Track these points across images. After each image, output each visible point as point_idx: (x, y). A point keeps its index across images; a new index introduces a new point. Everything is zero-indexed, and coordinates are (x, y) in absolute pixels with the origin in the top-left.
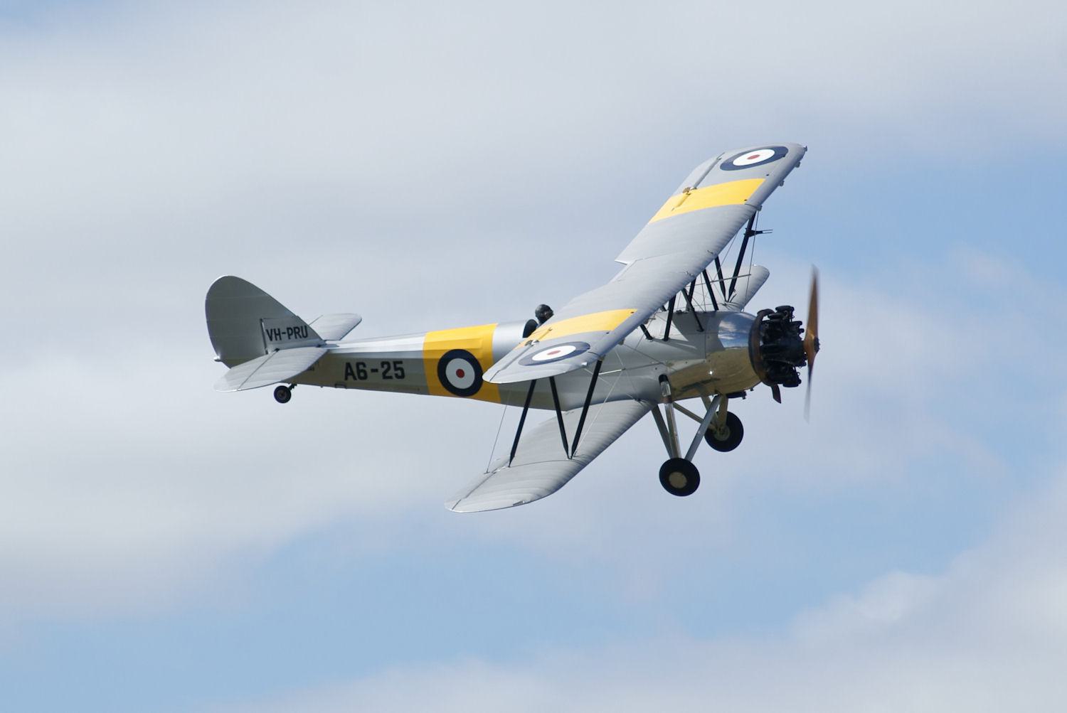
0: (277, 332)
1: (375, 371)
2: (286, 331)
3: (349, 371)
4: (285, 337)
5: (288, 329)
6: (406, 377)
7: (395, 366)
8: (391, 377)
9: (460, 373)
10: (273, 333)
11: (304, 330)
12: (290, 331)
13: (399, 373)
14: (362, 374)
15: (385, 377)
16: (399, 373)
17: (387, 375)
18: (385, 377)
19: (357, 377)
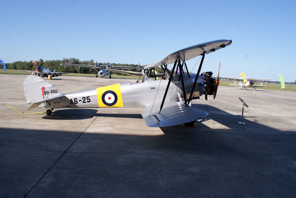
0: (47, 92)
1: (81, 100)
2: (50, 91)
3: (72, 102)
4: (50, 93)
8: (86, 102)
9: (110, 98)
10: (46, 93)
11: (56, 91)
12: (52, 91)
13: (89, 100)
14: (76, 102)
15: (84, 102)
16: (89, 100)
17: (84, 102)
18: (84, 102)
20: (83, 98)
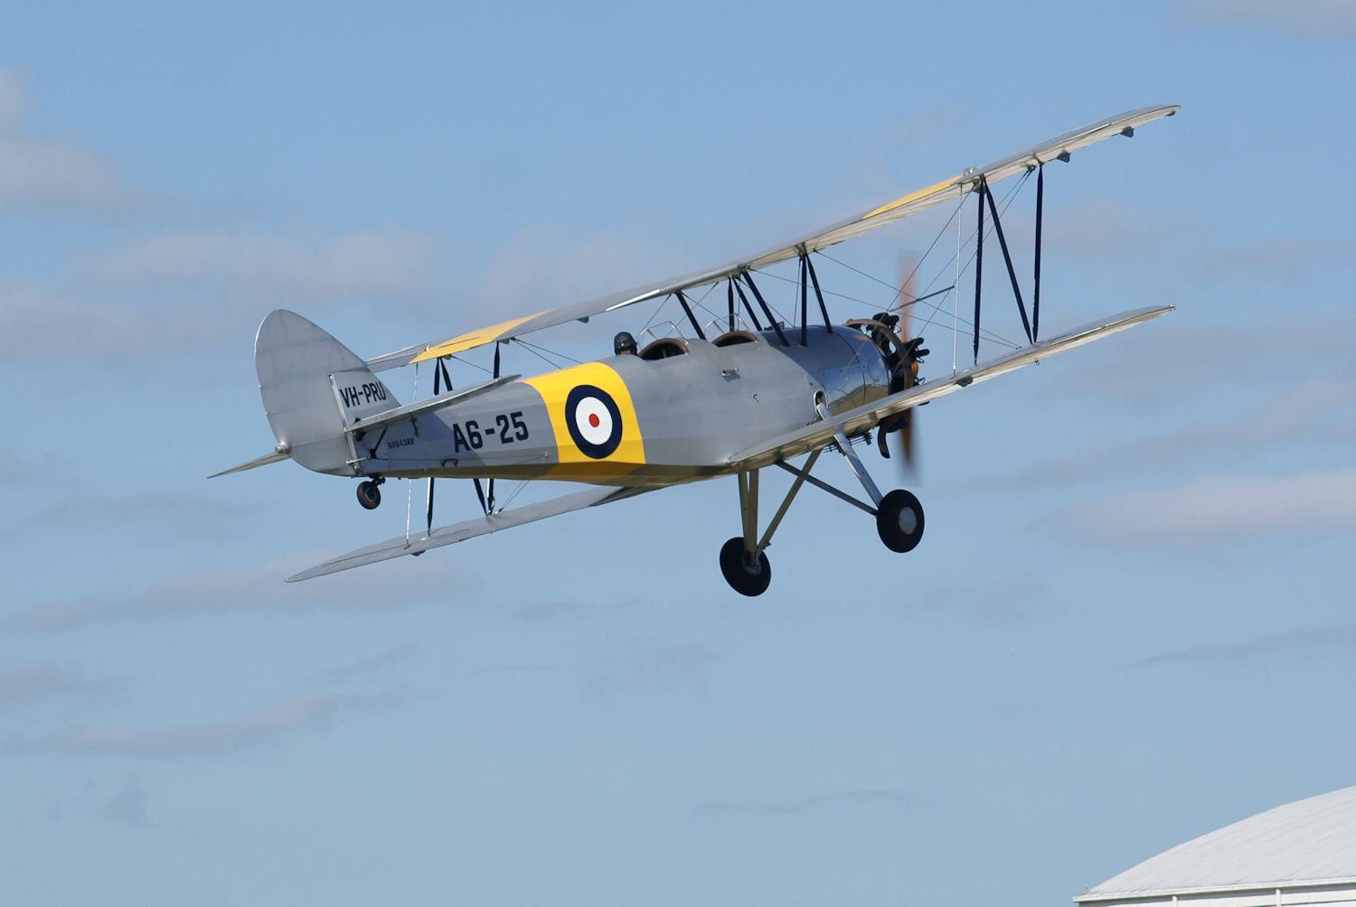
0: (353, 393)
1: (490, 432)
2: (362, 390)
4: (362, 398)
5: (364, 386)
6: (529, 435)
7: (514, 421)
8: (511, 440)
9: (594, 421)
13: (520, 430)
14: (476, 440)
15: (504, 441)
16: (522, 433)
17: (506, 436)
18: (504, 441)
19: (470, 446)
20: (499, 419)
